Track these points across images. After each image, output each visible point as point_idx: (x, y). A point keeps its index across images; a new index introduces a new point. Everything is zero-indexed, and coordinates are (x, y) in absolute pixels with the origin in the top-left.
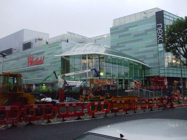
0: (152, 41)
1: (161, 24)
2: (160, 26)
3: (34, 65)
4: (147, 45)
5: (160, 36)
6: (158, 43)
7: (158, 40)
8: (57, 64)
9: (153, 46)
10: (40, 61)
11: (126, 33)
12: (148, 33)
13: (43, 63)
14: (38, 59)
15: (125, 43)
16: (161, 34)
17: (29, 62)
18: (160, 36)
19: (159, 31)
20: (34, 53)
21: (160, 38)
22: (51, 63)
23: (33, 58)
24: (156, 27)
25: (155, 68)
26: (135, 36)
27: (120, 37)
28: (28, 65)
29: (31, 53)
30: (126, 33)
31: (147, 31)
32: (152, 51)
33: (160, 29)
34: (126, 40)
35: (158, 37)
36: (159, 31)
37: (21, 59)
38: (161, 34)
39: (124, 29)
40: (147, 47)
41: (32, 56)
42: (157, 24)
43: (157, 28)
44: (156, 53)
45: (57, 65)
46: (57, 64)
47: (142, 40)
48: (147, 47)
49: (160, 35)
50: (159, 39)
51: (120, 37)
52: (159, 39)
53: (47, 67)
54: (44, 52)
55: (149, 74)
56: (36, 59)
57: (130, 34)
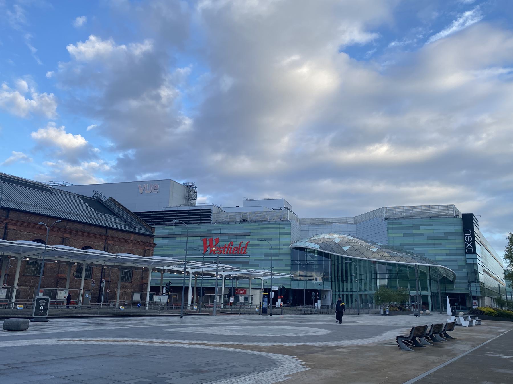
0: (455, 249)
1: (470, 230)
2: (469, 232)
3: (222, 254)
4: (448, 252)
5: (469, 245)
6: (466, 253)
7: (466, 249)
8: (280, 258)
9: (457, 254)
10: (237, 249)
11: (415, 231)
12: (449, 237)
13: (245, 253)
14: (232, 243)
15: (414, 244)
16: (471, 242)
17: (206, 247)
18: (469, 245)
19: (467, 238)
20: (222, 232)
21: (469, 247)
22: (266, 255)
23: (217, 241)
24: (461, 231)
25: (460, 283)
26: (429, 238)
27: (405, 235)
28: (203, 252)
29: (213, 232)
30: (415, 231)
31: (446, 235)
32: (456, 261)
33: (468, 236)
34: (415, 242)
35: (466, 245)
36: (467, 238)
37: (178, 239)
38: (471, 242)
39: (412, 226)
40: (447, 254)
41: (214, 238)
42: (464, 229)
43: (464, 234)
44: (462, 264)
45: (282, 260)
46: (281, 258)
47: (440, 244)
48: (447, 254)
49: (469, 243)
50: (467, 248)
51: (405, 235)
52: (467, 248)
53: (255, 260)
54: (249, 234)
55: (452, 290)
56: (227, 243)
57: (421, 235)
